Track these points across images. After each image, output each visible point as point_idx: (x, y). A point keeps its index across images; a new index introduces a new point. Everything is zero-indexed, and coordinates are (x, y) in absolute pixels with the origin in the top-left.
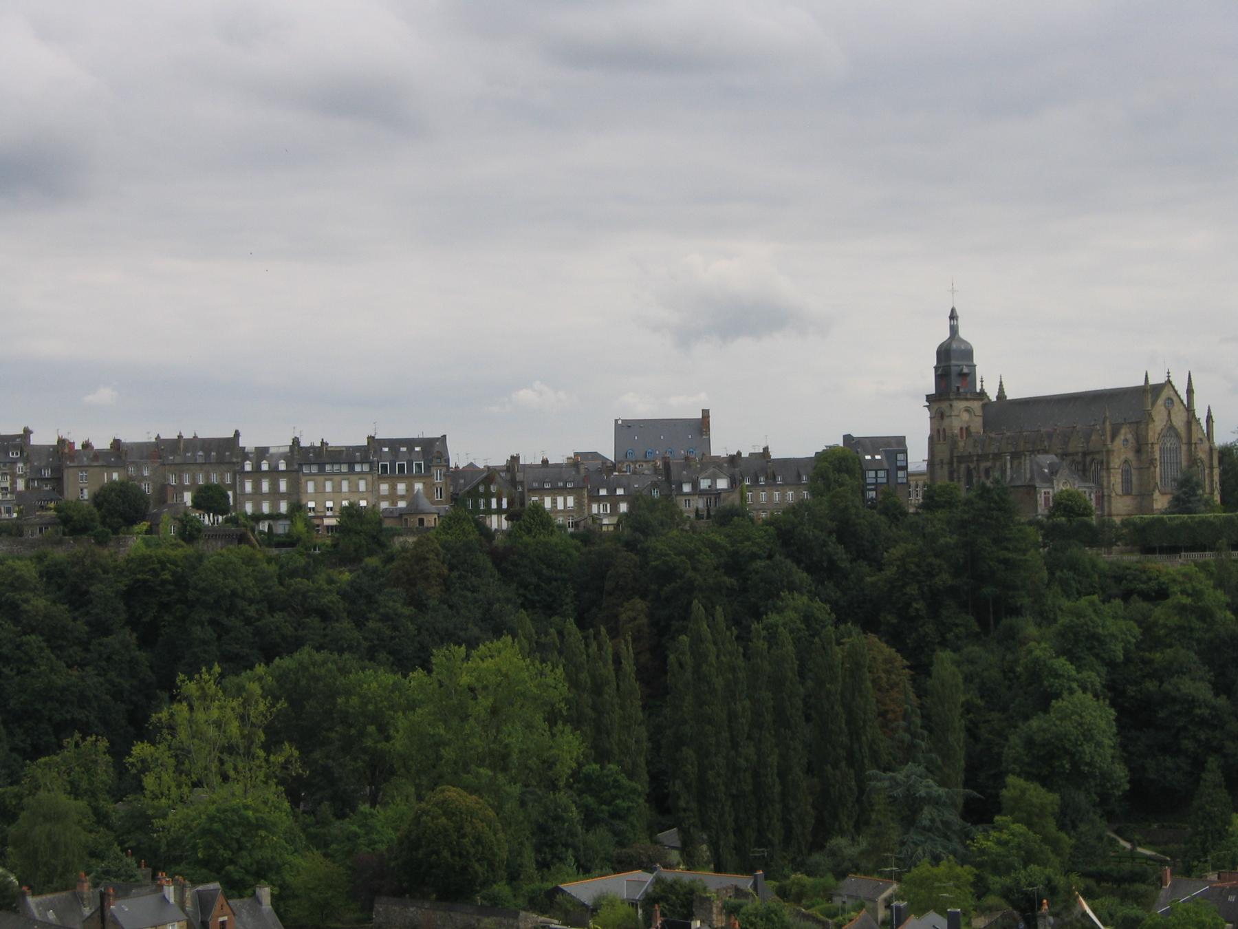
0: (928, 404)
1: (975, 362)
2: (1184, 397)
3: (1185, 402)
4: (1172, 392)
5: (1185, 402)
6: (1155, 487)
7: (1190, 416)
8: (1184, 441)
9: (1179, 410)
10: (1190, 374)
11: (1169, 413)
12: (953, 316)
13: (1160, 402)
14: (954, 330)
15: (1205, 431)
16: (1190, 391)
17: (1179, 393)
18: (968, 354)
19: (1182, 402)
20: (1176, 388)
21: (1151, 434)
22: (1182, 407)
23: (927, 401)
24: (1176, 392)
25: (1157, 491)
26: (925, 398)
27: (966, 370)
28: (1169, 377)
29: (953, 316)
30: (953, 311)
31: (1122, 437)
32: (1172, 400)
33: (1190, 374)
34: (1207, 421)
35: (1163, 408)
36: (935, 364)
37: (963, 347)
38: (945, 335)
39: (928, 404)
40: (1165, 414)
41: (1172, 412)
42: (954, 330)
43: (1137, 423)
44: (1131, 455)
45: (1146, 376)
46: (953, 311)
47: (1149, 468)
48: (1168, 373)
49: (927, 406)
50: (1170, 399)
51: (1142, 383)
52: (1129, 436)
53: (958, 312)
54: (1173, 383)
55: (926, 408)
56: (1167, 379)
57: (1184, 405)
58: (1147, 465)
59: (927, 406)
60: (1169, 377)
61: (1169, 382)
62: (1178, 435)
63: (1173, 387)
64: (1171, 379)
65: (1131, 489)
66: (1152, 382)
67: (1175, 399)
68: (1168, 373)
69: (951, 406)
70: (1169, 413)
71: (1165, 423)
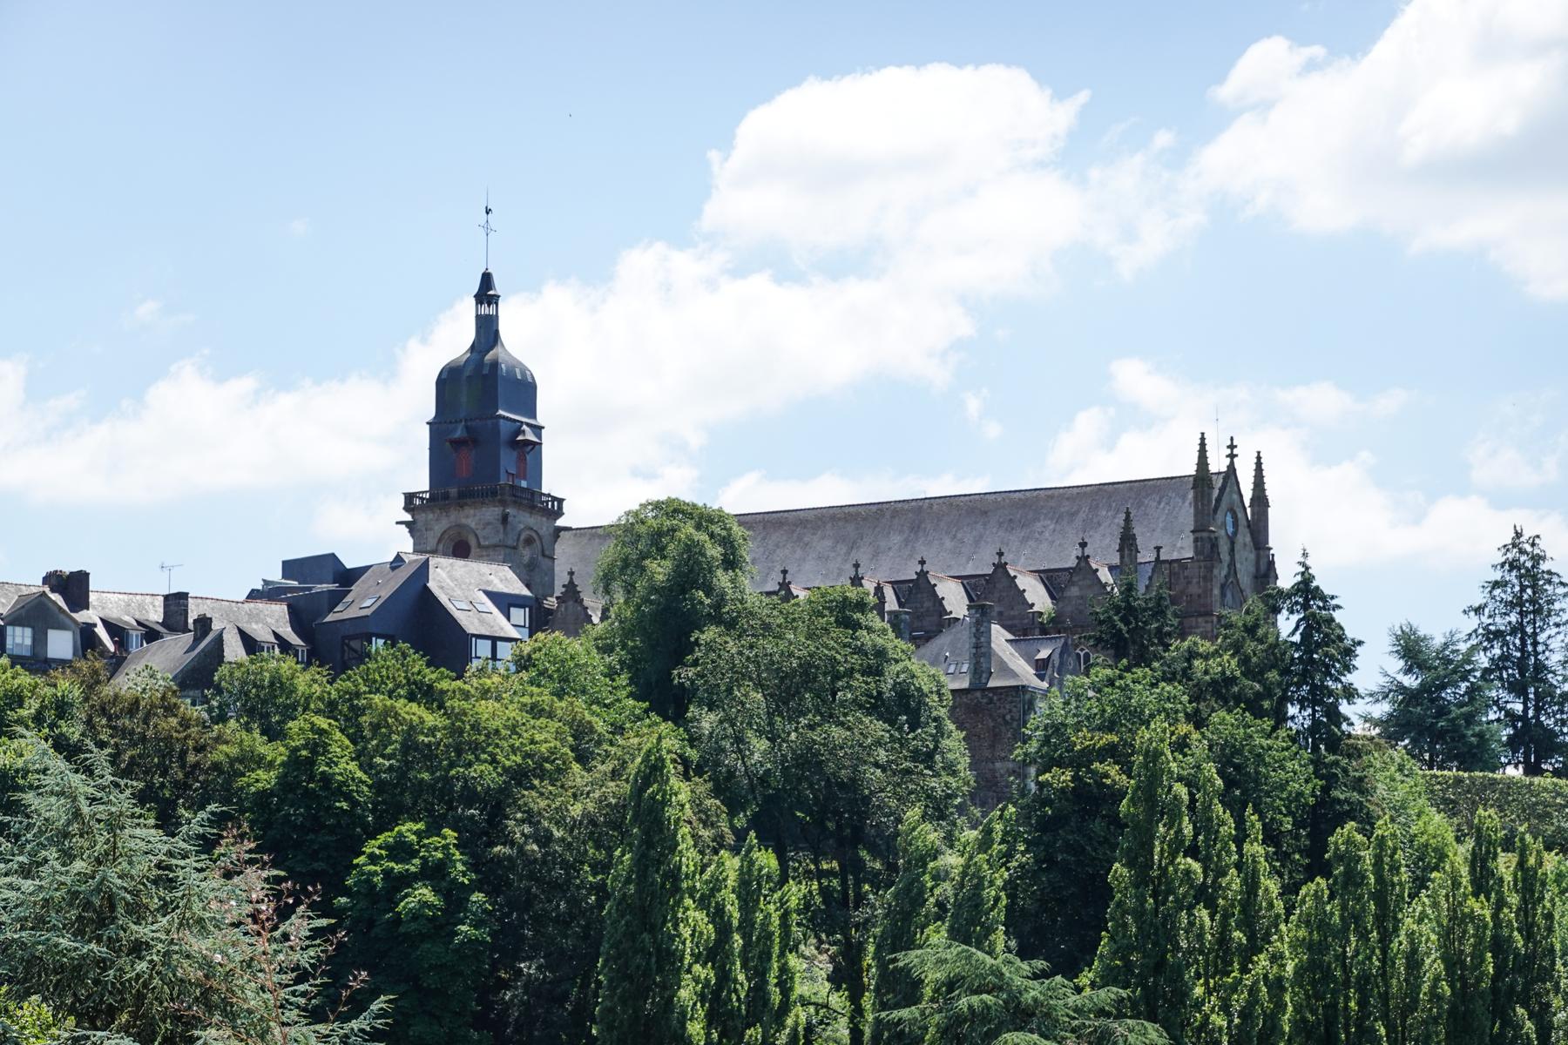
0: (408, 517)
4: (1235, 497)
9: (1245, 545)
14: (487, 330)
16: (1260, 499)
18: (524, 391)
23: (407, 509)
26: (401, 502)
28: (1232, 456)
29: (486, 293)
30: (487, 280)
33: (1259, 458)
36: (431, 412)
39: (408, 517)
42: (487, 330)
46: (487, 280)
48: (1232, 447)
49: (407, 524)
53: (499, 287)
55: (404, 529)
59: (407, 524)
60: (1232, 456)
68: (1232, 447)
69: (505, 519)
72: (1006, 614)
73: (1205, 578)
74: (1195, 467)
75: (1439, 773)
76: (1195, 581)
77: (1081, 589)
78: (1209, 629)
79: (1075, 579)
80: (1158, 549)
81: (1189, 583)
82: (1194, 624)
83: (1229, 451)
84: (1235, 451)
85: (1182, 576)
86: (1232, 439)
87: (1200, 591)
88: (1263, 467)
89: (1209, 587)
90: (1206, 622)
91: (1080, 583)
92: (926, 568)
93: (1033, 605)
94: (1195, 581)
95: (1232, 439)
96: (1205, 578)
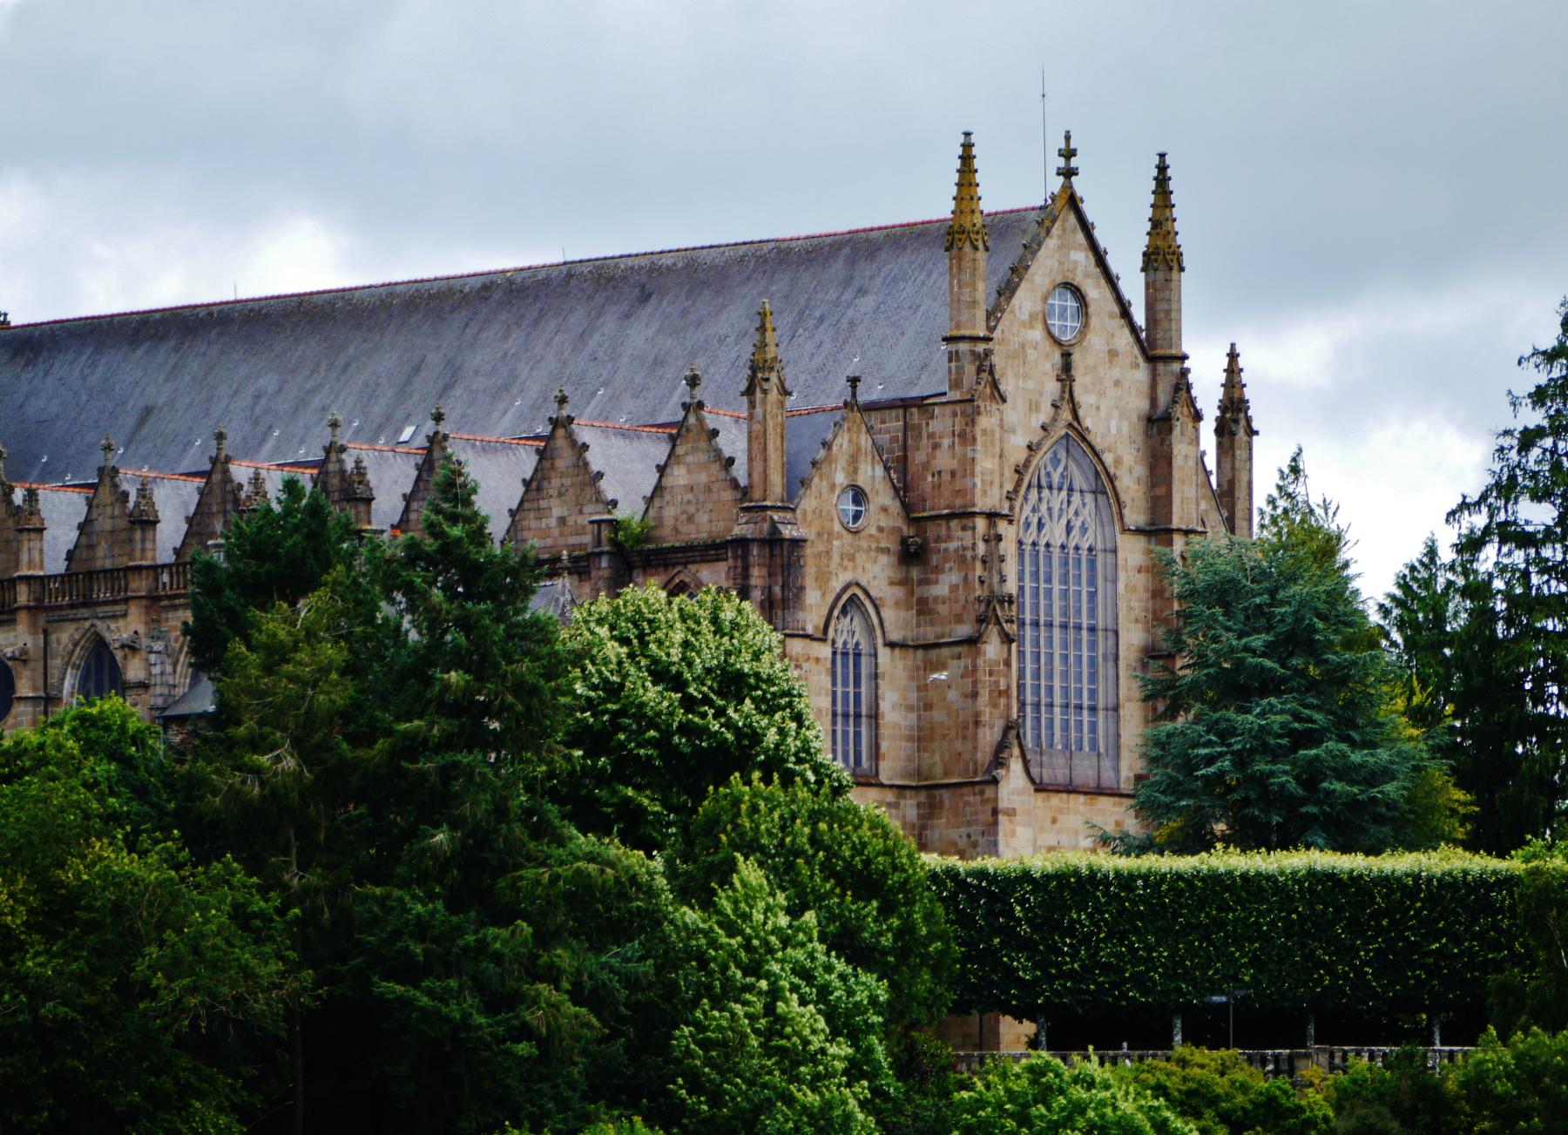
2: (1134, 287)
3: (1140, 318)
4: (1081, 258)
5: (1140, 318)
6: (1002, 746)
7: (1163, 398)
8: (1135, 515)
9: (1113, 353)
10: (1162, 168)
11: (1067, 367)
13: (1025, 301)
19: (1125, 313)
21: (986, 463)
22: (1124, 339)
25: (1016, 766)
28: (1068, 173)
31: (840, 478)
33: (1162, 168)
35: (1037, 334)
43: (905, 404)
44: (877, 574)
47: (973, 642)
48: (1069, 154)
51: (939, 205)
52: (871, 475)
56: (1057, 183)
58: (964, 630)
60: (1068, 173)
62: (1104, 485)
63: (1086, 228)
65: (876, 755)
66: (994, 197)
67: (1096, 292)
68: (1069, 154)
70: (1066, 372)
71: (1046, 413)
72: (570, 522)
73: (962, 435)
74: (952, 205)
75: (953, 861)
76: (946, 442)
77: (689, 472)
78: (968, 543)
79: (680, 450)
80: (854, 381)
81: (936, 446)
82: (944, 532)
83: (1061, 162)
84: (1074, 162)
85: (924, 434)
86: (1068, 138)
87: (954, 464)
88: (1172, 185)
89: (970, 455)
90: (964, 528)
91: (689, 459)
92: (443, 428)
93: (614, 503)
94: (946, 442)
95: (1068, 138)
96: (962, 435)
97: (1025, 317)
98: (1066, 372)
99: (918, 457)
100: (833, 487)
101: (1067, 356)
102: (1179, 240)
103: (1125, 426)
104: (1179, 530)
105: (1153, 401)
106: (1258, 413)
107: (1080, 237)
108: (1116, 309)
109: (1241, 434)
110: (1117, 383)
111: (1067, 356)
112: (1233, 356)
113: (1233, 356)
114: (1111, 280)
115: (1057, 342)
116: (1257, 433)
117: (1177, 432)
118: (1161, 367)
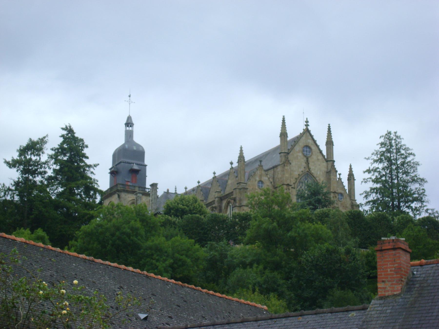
1: (146, 162)
2: (323, 148)
3: (325, 153)
4: (310, 141)
5: (325, 153)
7: (329, 168)
9: (318, 160)
10: (329, 127)
11: (307, 161)
12: (129, 124)
14: (129, 135)
15: (346, 188)
16: (330, 143)
17: (318, 143)
19: (321, 152)
20: (315, 138)
22: (320, 157)
24: (315, 142)
27: (135, 167)
28: (307, 125)
29: (129, 124)
30: (129, 118)
31: (258, 179)
32: (309, 148)
33: (329, 127)
34: (349, 179)
35: (300, 154)
37: (135, 148)
38: (120, 141)
40: (303, 160)
41: (309, 159)
42: (129, 135)
45: (284, 121)
46: (129, 118)
48: (307, 122)
50: (307, 146)
54: (312, 133)
56: (305, 127)
57: (323, 156)
60: (307, 125)
61: (307, 131)
63: (312, 136)
64: (309, 128)
67: (314, 148)
68: (307, 122)
70: (307, 161)
81: (278, 174)
83: (306, 124)
86: (307, 119)
95: (307, 119)
97: (297, 151)
98: (307, 162)
99: (276, 176)
100: (256, 180)
101: (307, 159)
102: (333, 140)
103: (321, 173)
104: (332, 192)
105: (327, 168)
106: (356, 177)
107: (310, 137)
108: (319, 151)
109: (352, 180)
110: (319, 165)
111: (307, 159)
112: (351, 166)
113: (351, 166)
114: (318, 146)
115: (305, 156)
116: (355, 180)
117: (332, 174)
118: (329, 163)
